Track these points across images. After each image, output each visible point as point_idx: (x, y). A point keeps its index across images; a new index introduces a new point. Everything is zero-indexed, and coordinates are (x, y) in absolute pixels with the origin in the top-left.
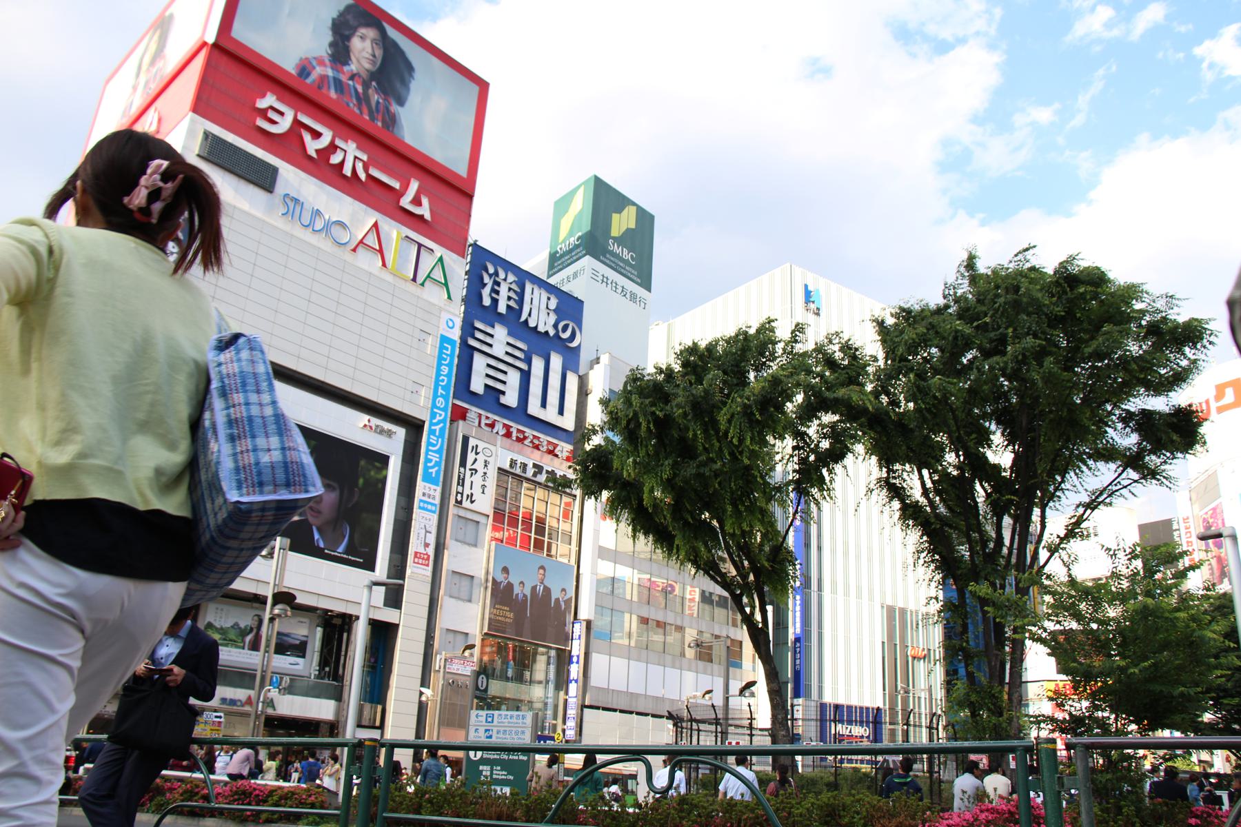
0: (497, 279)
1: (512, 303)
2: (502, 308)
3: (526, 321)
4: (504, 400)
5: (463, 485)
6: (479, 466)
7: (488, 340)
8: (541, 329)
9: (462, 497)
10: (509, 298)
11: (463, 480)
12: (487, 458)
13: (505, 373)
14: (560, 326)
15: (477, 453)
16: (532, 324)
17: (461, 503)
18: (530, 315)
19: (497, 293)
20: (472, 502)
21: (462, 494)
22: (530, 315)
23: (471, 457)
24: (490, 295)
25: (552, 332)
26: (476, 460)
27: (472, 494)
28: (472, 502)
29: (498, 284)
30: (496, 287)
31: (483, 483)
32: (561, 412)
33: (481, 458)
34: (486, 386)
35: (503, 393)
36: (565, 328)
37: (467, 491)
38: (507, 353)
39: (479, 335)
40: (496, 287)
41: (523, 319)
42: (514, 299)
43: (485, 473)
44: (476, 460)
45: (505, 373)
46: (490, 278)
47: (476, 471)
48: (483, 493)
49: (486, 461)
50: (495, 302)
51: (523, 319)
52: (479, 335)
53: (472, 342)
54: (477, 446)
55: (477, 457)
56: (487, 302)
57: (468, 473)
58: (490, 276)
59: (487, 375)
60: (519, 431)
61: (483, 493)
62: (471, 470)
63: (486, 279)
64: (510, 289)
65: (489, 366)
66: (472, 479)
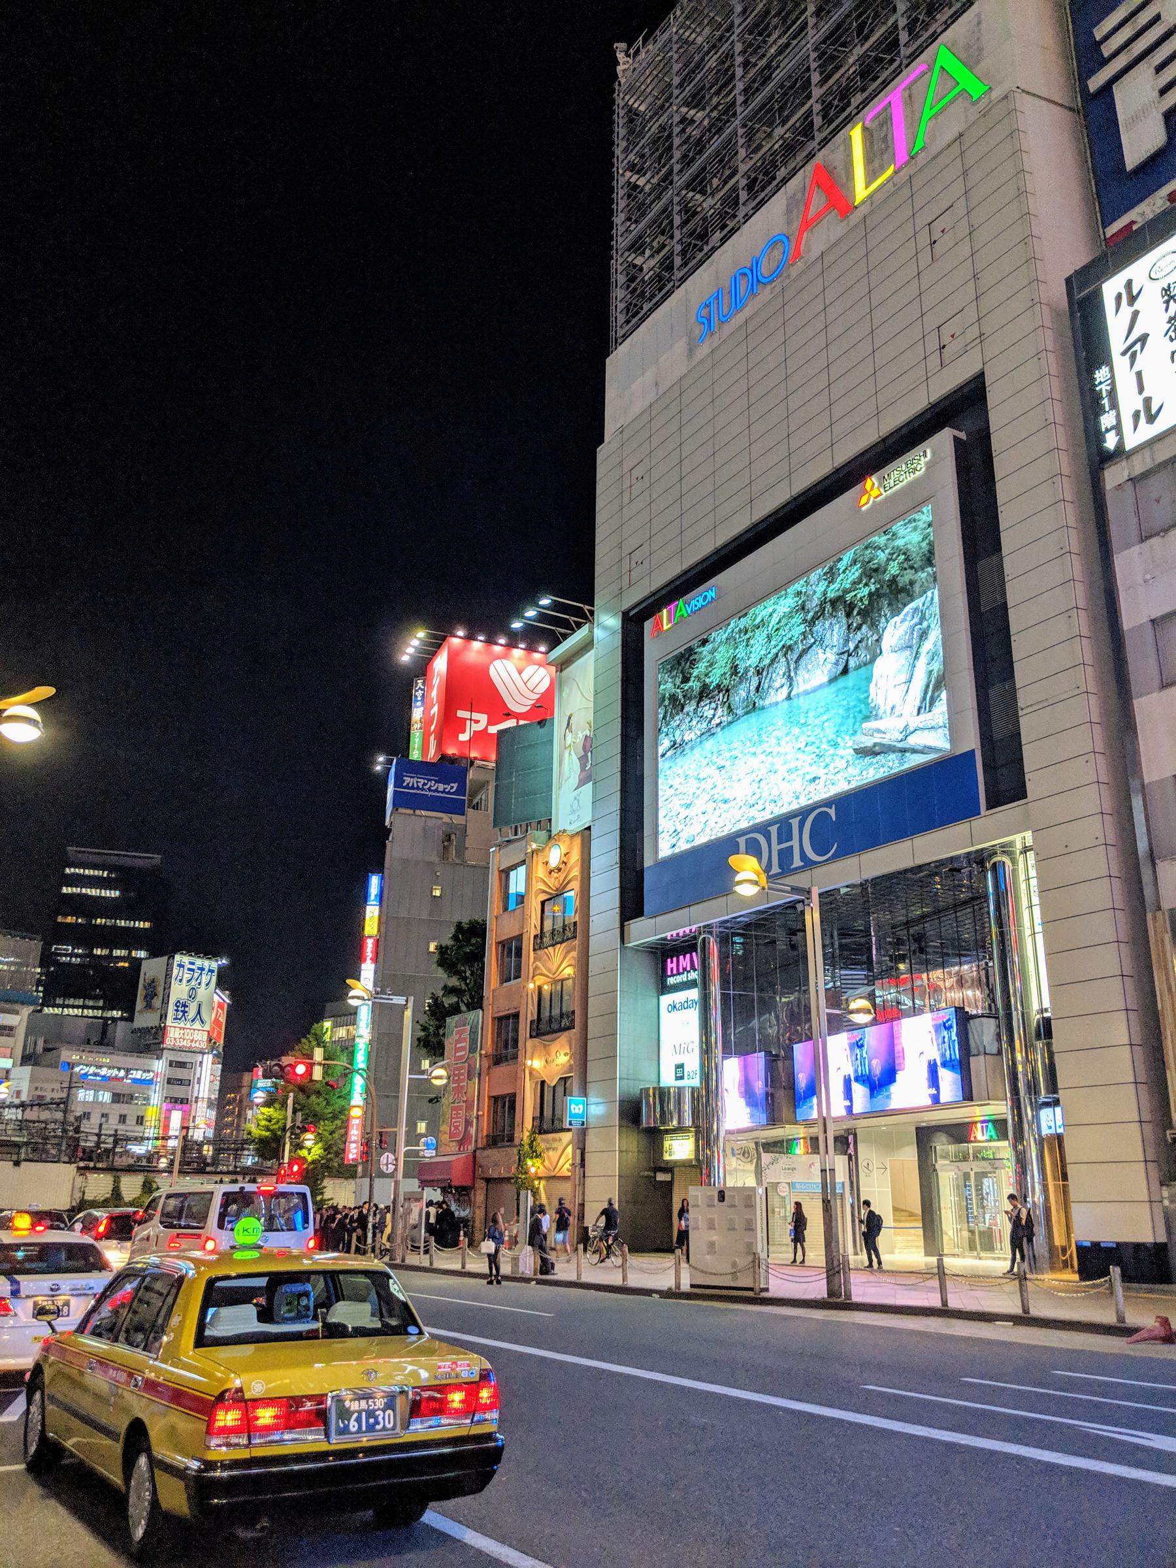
5: (1114, 405)
11: (1112, 393)
15: (1132, 299)
21: (1118, 428)
23: (1116, 325)
26: (1136, 314)
27: (1147, 402)
28: (1151, 419)
37: (1129, 401)
44: (1136, 314)
47: (1143, 339)
54: (1129, 284)
55: (1137, 305)
57: (1120, 363)
62: (1124, 353)
66: (1136, 368)
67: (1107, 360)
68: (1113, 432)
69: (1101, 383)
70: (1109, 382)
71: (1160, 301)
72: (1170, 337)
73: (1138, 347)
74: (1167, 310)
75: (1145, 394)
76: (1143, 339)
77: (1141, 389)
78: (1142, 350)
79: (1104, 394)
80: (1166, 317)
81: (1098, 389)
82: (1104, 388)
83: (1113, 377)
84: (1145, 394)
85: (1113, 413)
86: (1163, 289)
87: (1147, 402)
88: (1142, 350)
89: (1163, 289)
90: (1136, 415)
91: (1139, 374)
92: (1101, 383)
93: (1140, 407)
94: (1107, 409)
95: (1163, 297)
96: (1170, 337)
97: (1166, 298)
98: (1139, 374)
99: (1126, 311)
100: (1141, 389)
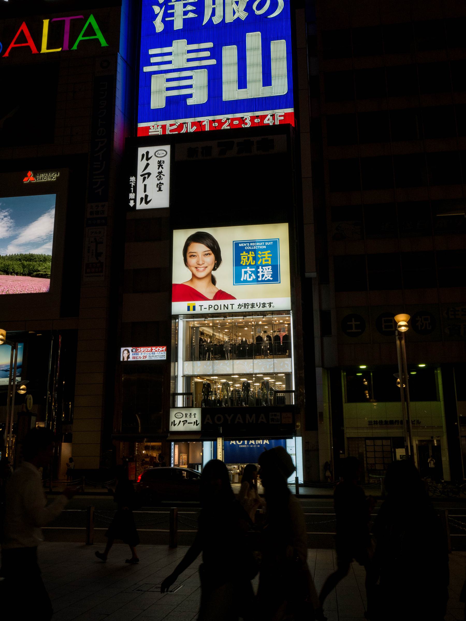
0: (170, 4)
1: (191, 15)
2: (178, 25)
3: (210, 20)
4: (190, 102)
5: (135, 192)
6: (153, 169)
7: (167, 58)
8: (229, 19)
9: (135, 201)
10: (185, 13)
11: (135, 187)
12: (160, 159)
13: (190, 78)
14: (254, 6)
15: (148, 159)
16: (217, 20)
17: (135, 206)
18: (213, 14)
19: (172, 15)
20: (147, 203)
21: (135, 200)
22: (213, 14)
24: (163, 21)
25: (243, 15)
26: (148, 165)
27: (146, 196)
28: (147, 203)
29: (172, 7)
30: (169, 11)
31: (158, 182)
32: (267, 81)
33: (154, 162)
34: (169, 100)
35: (190, 96)
36: (260, 7)
37: (140, 194)
38: (189, 60)
39: (153, 60)
40: (169, 11)
41: (205, 21)
42: (192, 11)
43: (160, 173)
44: (148, 165)
45: (190, 78)
46: (161, 9)
47: (149, 174)
48: (160, 190)
49: (159, 162)
50: (169, 25)
51: (205, 21)
52: (153, 60)
53: (147, 69)
54: (147, 153)
55: (149, 162)
56: (159, 26)
57: (140, 179)
58: (161, 6)
59: (168, 89)
60: (211, 122)
61: (160, 190)
62: (142, 176)
63: (156, 9)
64: (185, 5)
65: (168, 80)
66: (145, 183)
67: (135, 174)
68: (133, 201)
69: (131, 182)
70: (135, 183)
71: (156, 165)
72: (158, 178)
73: (147, 176)
74: (159, 169)
75: (146, 193)
76: (149, 174)
77: (145, 191)
78: (147, 178)
79: (132, 187)
80: (158, 171)
81: (130, 183)
82: (133, 184)
83: (136, 182)
84: (146, 193)
85: (134, 194)
86: (159, 161)
87: (146, 196)
88: (147, 178)
89: (159, 161)
90: (142, 199)
91: (145, 186)
92: (131, 182)
93: (144, 197)
94: (132, 192)
95: (158, 164)
96: (158, 178)
97: (159, 164)
98: (145, 186)
99: (145, 162)
100: (145, 191)
